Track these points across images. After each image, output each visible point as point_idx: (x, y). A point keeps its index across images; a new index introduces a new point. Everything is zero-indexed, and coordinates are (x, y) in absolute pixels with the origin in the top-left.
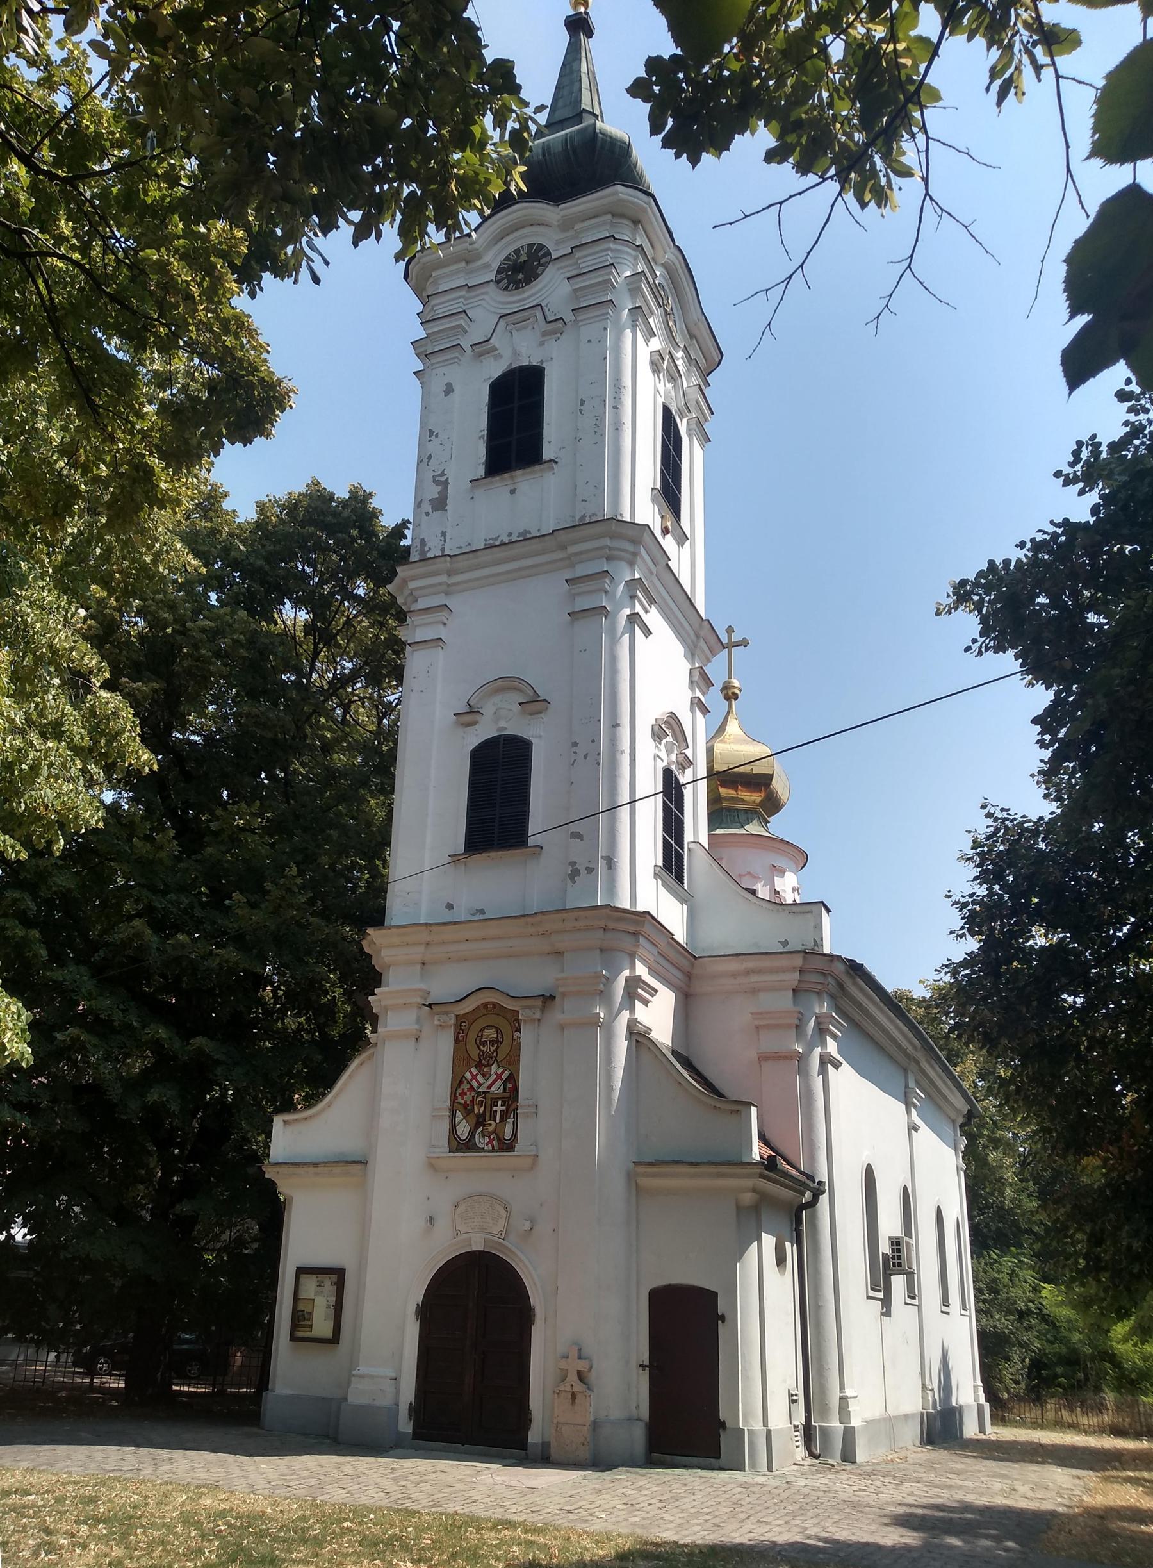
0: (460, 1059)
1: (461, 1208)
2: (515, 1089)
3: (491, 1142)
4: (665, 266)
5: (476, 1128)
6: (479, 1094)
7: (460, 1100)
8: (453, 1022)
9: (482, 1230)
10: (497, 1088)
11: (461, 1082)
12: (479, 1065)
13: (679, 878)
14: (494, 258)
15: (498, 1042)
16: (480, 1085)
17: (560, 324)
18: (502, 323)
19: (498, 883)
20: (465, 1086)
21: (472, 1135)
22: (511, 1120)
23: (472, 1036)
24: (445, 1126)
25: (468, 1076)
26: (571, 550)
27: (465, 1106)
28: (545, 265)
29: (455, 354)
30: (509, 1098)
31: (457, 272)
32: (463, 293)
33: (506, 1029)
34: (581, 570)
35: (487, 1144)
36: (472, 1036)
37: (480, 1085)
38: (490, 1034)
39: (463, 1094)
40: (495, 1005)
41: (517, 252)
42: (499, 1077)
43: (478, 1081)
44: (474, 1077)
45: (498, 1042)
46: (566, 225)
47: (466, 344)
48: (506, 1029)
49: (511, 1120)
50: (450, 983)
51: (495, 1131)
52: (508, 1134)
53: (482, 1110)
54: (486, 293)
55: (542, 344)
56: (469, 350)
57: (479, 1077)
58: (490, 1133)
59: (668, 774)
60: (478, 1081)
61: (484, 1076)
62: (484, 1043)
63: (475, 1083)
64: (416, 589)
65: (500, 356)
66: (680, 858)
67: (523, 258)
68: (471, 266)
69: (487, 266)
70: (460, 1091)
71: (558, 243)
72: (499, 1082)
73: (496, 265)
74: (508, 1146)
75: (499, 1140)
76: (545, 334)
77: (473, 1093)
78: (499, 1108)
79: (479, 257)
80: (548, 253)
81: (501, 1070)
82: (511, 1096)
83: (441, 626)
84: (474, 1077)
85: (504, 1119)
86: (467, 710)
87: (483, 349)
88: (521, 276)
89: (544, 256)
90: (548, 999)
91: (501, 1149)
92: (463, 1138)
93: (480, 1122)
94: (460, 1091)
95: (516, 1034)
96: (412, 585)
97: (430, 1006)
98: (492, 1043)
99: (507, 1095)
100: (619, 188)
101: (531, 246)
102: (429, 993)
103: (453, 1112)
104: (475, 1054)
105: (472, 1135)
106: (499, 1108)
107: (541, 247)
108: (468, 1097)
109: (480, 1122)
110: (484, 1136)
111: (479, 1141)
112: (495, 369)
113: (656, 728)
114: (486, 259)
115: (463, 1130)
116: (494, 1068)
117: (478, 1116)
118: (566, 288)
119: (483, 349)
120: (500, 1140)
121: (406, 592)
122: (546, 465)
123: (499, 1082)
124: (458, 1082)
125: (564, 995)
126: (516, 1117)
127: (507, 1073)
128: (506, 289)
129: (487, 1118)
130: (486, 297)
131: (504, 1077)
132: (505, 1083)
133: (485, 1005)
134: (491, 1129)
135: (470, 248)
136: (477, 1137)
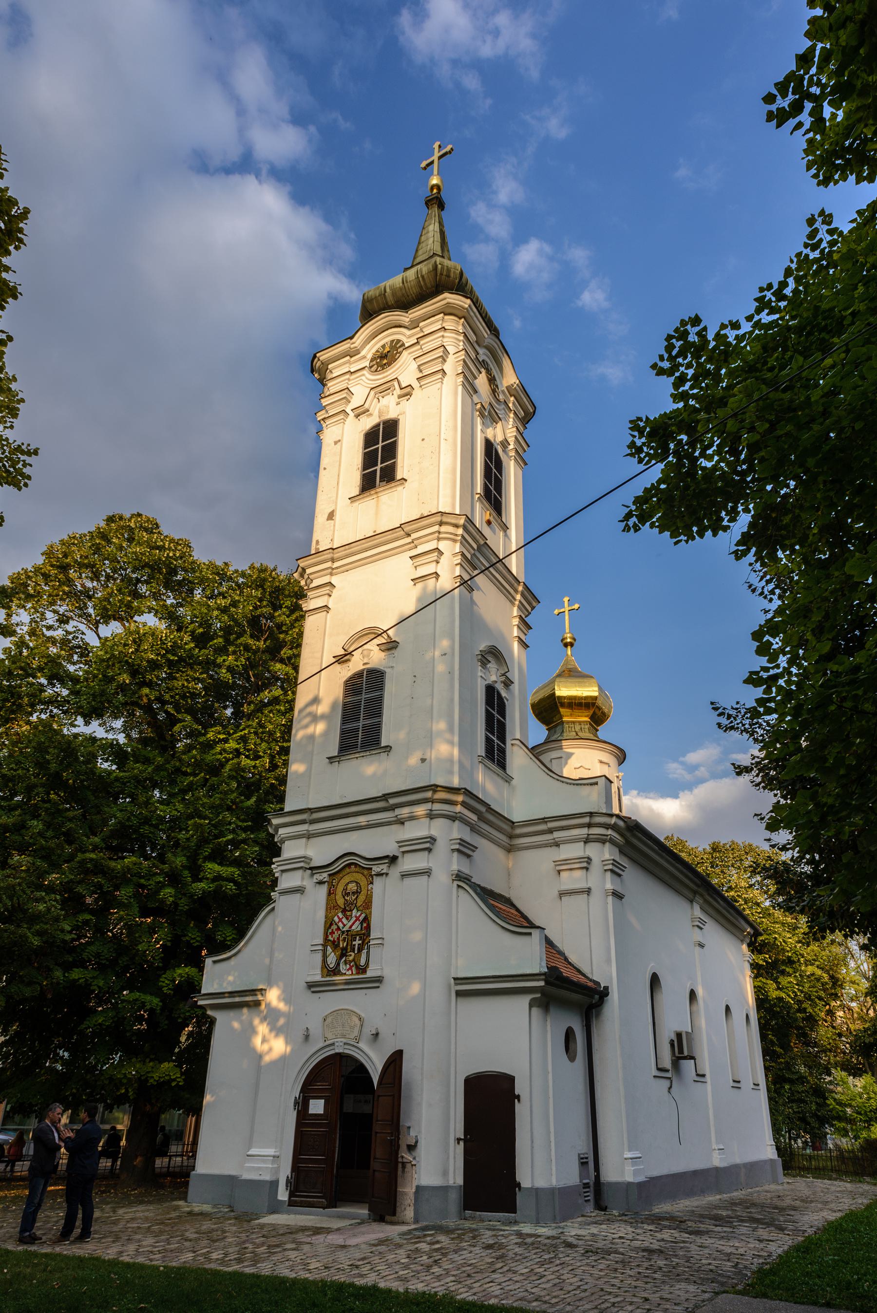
0: (331, 906)
1: (329, 1020)
2: (368, 927)
3: (351, 968)
4: (487, 348)
5: (341, 958)
6: (343, 932)
7: (330, 938)
9: (344, 1036)
10: (356, 927)
11: (331, 924)
12: (344, 911)
13: (502, 765)
14: (369, 351)
15: (357, 893)
17: (408, 389)
18: (372, 393)
19: (369, 775)
20: (334, 927)
22: (365, 951)
23: (340, 888)
24: (319, 957)
25: (336, 919)
26: (414, 536)
27: (334, 942)
28: (401, 353)
29: (341, 416)
30: (364, 934)
31: (344, 364)
32: (347, 376)
33: (363, 882)
34: (421, 549)
36: (340, 888)
37: (345, 926)
38: (352, 887)
39: (333, 933)
40: (356, 865)
41: (383, 346)
42: (357, 919)
44: (340, 920)
45: (357, 893)
46: (414, 325)
47: (348, 410)
48: (363, 882)
50: (323, 850)
51: (354, 960)
52: (363, 962)
53: (345, 944)
54: (363, 375)
55: (398, 404)
56: (352, 414)
57: (344, 920)
58: (351, 962)
59: (490, 690)
61: (347, 919)
63: (341, 925)
64: (311, 574)
65: (371, 415)
66: (503, 752)
67: (388, 349)
68: (353, 359)
69: (364, 357)
70: (330, 931)
71: (410, 337)
73: (370, 356)
75: (357, 967)
76: (400, 397)
78: (357, 942)
79: (358, 352)
80: (403, 345)
81: (359, 913)
82: (365, 934)
83: (327, 597)
84: (340, 920)
85: (360, 950)
86: (343, 652)
87: (361, 412)
88: (385, 361)
89: (400, 347)
90: (393, 860)
91: (358, 973)
93: (343, 954)
94: (330, 931)
95: (370, 886)
96: (308, 571)
97: (311, 869)
98: (353, 893)
100: (446, 295)
101: (393, 341)
102: (311, 860)
103: (324, 946)
104: (341, 902)
105: (338, 965)
106: (357, 942)
107: (399, 341)
108: (336, 936)
109: (343, 954)
110: (346, 964)
111: (343, 968)
112: (368, 423)
113: (480, 657)
114: (363, 353)
115: (332, 959)
116: (354, 912)
117: (343, 949)
118: (414, 366)
119: (361, 412)
120: (357, 967)
121: (306, 576)
122: (398, 483)
123: (358, 922)
124: (329, 924)
125: (404, 852)
126: (369, 948)
127: (363, 915)
128: (376, 371)
130: (363, 378)
131: (361, 918)
132: (361, 923)
133: (349, 865)
134: (351, 958)
135: (352, 346)
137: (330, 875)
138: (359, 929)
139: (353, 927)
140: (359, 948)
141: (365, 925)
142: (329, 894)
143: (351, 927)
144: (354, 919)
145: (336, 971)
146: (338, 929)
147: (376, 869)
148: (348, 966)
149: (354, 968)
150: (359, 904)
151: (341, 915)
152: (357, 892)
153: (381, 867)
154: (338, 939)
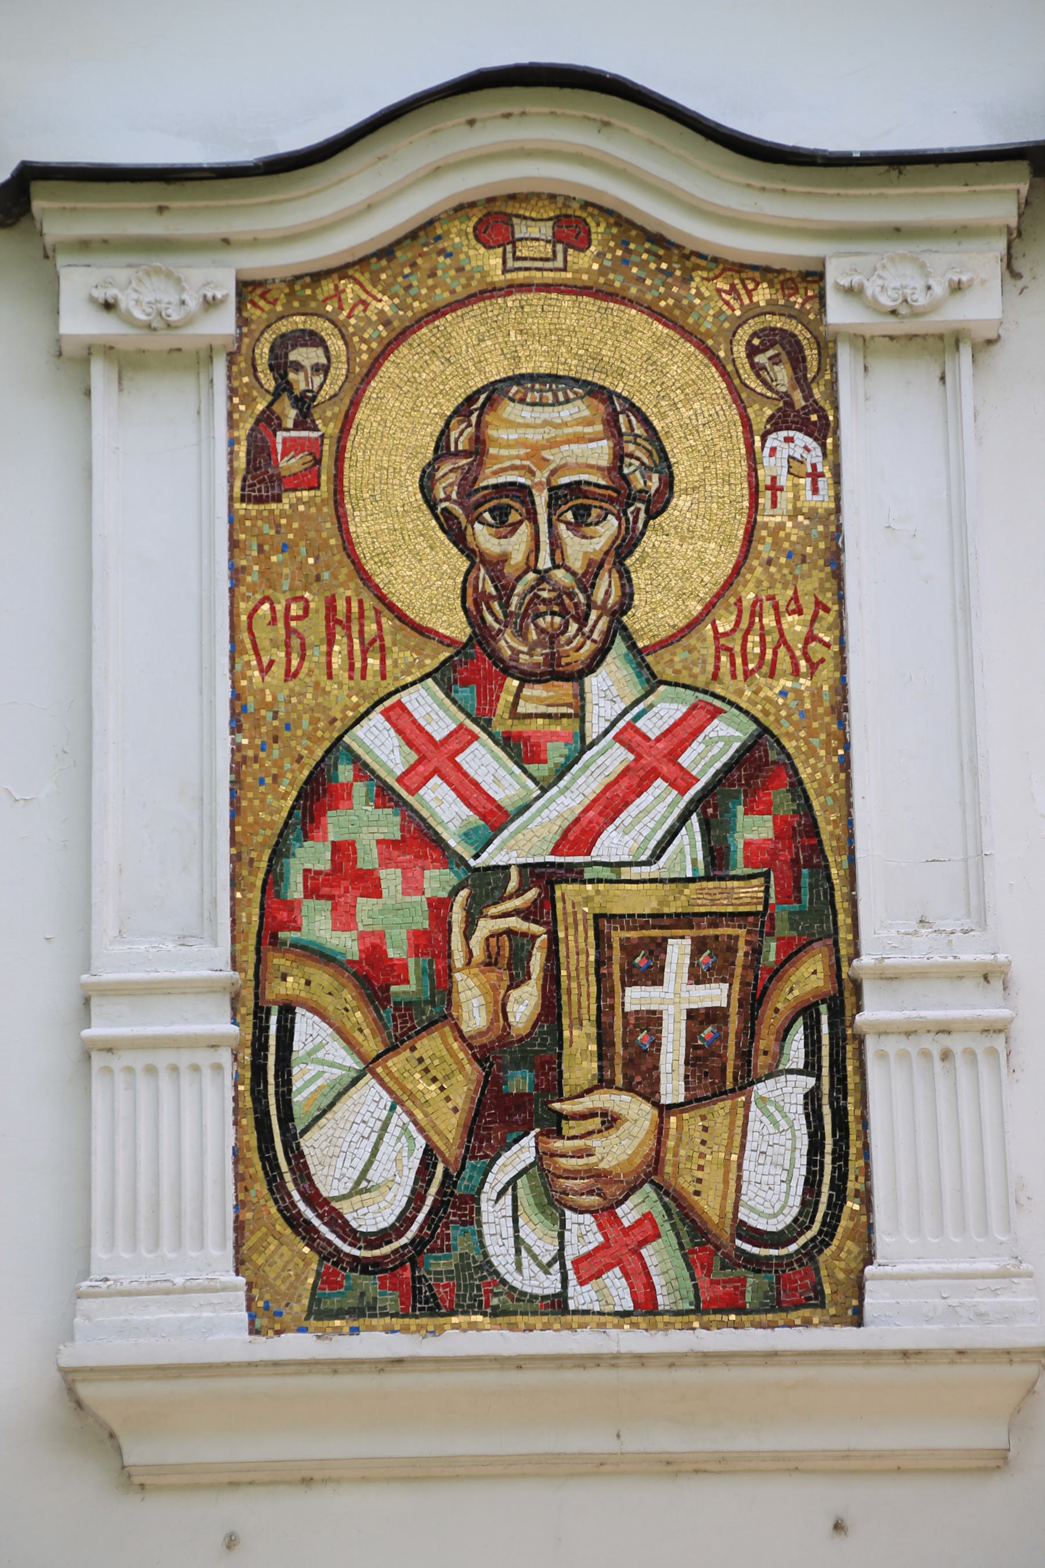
3: (621, 1251)
6: (485, 886)
8: (223, 324)
11: (317, 796)
12: (471, 667)
15: (633, 494)
16: (495, 818)
20: (362, 825)
21: (447, 1199)
22: (784, 1095)
25: (380, 745)
27: (372, 975)
30: (759, 922)
35: (590, 1267)
36: (393, 437)
37: (495, 818)
38: (549, 441)
39: (345, 880)
42: (652, 762)
43: (468, 790)
49: (784, 1095)
51: (652, 1171)
52: (770, 1189)
53: (524, 1006)
60: (468, 790)
61: (521, 750)
62: (508, 503)
63: (443, 807)
70: (312, 856)
72: (659, 804)
74: (796, 1272)
75: (696, 1235)
77: (437, 881)
78: (676, 995)
84: (435, 757)
85: (723, 1069)
91: (717, 1305)
92: (372, 1215)
94: (312, 856)
98: (574, 501)
99: (747, 894)
106: (676, 995)
108: (394, 912)
110: (555, 1206)
111: (507, 1233)
115: (368, 1153)
116: (609, 689)
117: (491, 1053)
123: (659, 804)
129: (580, 1063)
132: (710, 807)
134: (616, 1151)
136: (494, 1215)
137: (248, 289)
138: (689, 850)
139: (613, 844)
140: (699, 1059)
141: (753, 828)
142: (259, 479)
143: (580, 835)
144: (613, 759)
145: (422, 1269)
146: (421, 841)
147: (866, 285)
148: (584, 1234)
149: (662, 1259)
150: (648, 620)
151: (434, 711)
152: (620, 494)
153: (945, 262)
154: (432, 943)
